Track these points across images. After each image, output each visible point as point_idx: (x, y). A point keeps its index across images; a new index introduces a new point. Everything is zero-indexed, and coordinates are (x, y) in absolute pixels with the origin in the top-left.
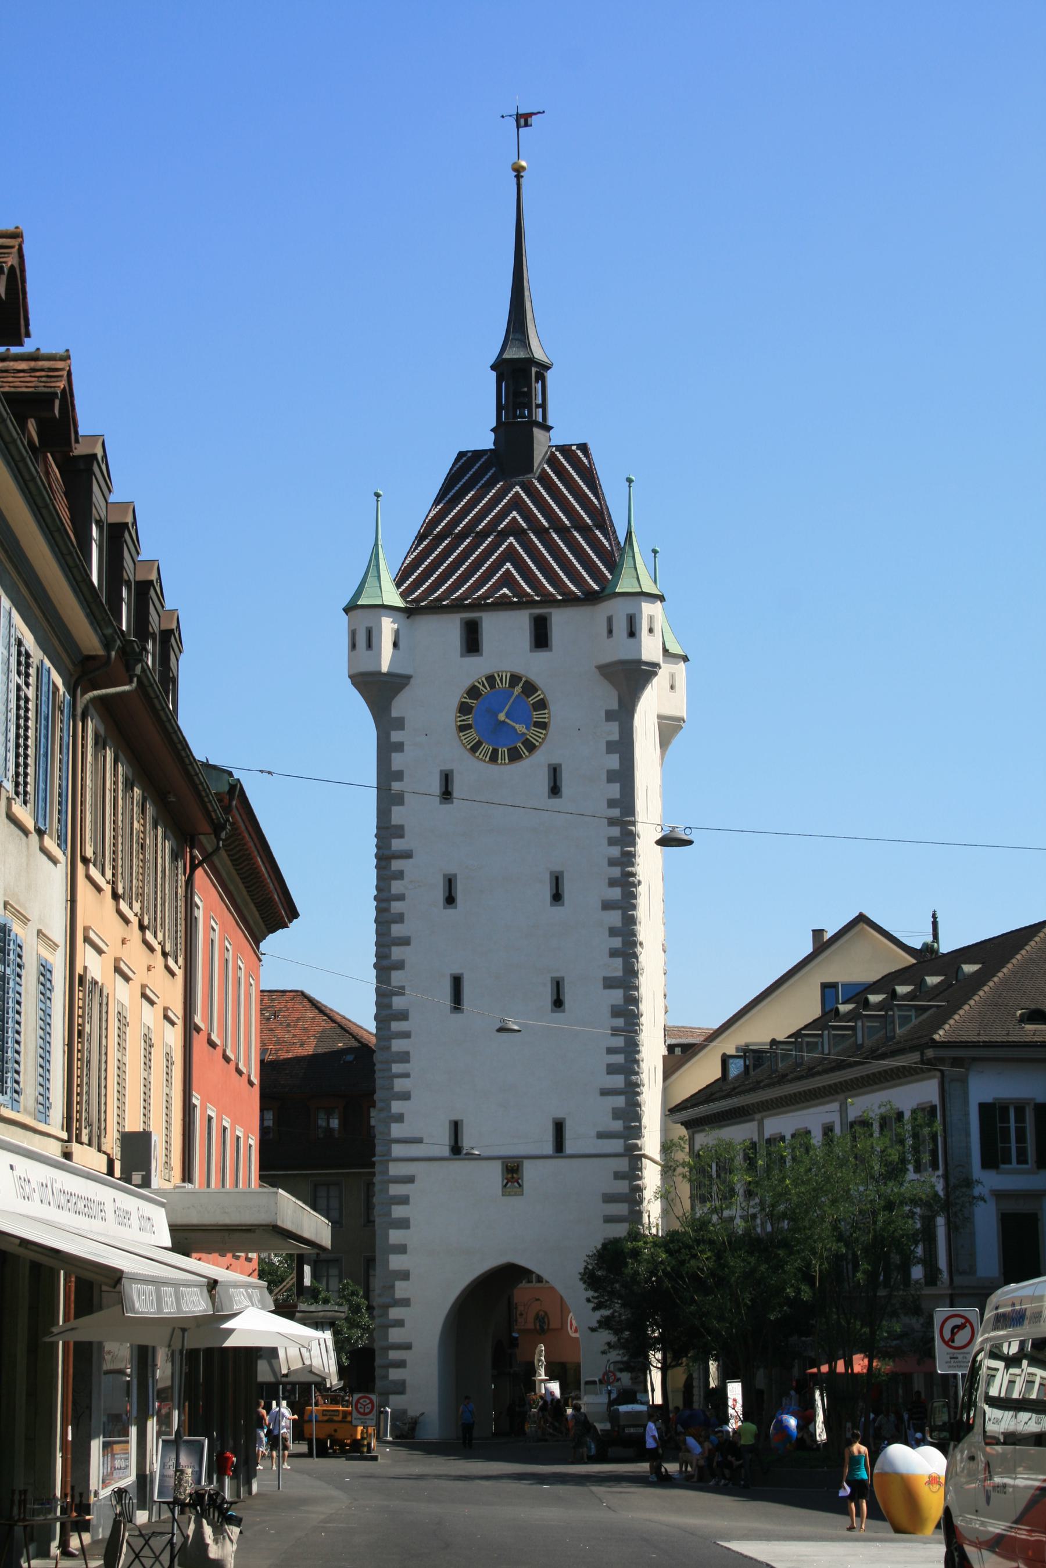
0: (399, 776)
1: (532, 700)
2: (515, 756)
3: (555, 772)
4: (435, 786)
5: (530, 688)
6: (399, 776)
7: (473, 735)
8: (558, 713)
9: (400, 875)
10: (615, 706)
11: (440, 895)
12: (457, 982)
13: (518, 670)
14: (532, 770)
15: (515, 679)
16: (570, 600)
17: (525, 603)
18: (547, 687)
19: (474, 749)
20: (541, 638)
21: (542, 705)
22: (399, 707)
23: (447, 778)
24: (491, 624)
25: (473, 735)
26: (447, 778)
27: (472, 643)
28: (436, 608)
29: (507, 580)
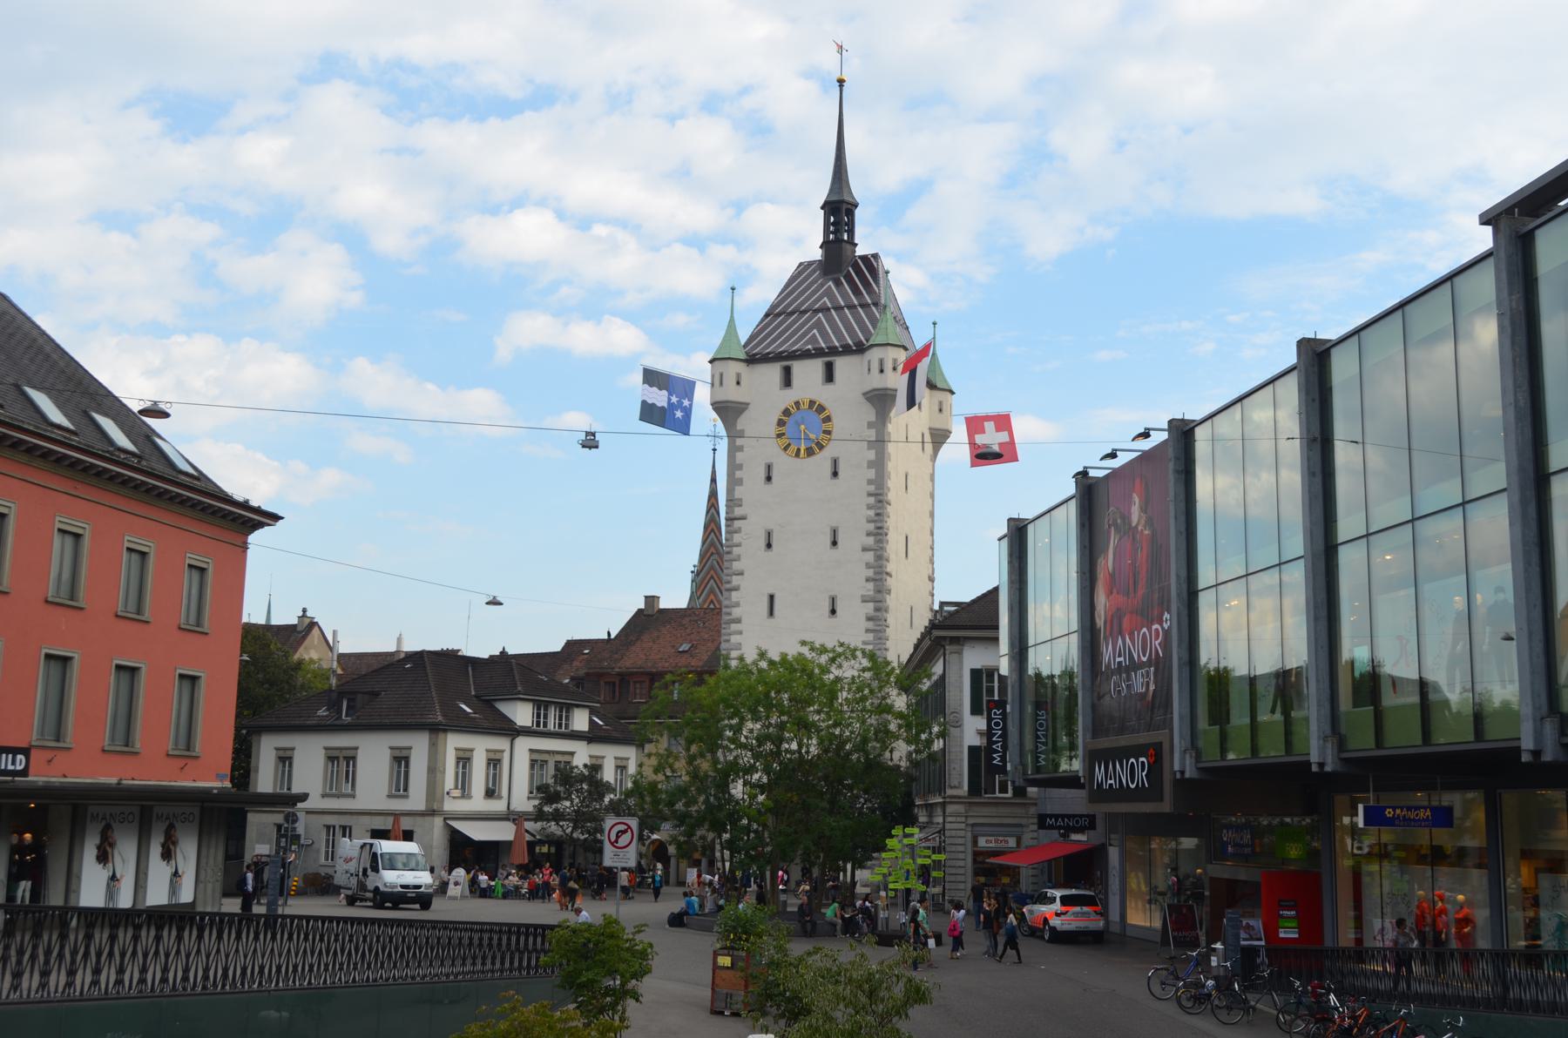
0: (740, 467)
1: (823, 416)
2: (810, 452)
3: (835, 462)
4: (763, 475)
5: (821, 409)
6: (740, 467)
7: (785, 441)
8: (838, 425)
9: (738, 531)
10: (873, 418)
11: (763, 543)
12: (772, 597)
13: (813, 397)
14: (822, 460)
15: (812, 403)
16: (846, 350)
17: (819, 353)
18: (832, 409)
19: (785, 449)
20: (829, 376)
21: (828, 419)
22: (742, 423)
23: (769, 467)
24: (799, 368)
25: (785, 441)
26: (769, 467)
27: (787, 381)
28: (765, 359)
29: (813, 340)
